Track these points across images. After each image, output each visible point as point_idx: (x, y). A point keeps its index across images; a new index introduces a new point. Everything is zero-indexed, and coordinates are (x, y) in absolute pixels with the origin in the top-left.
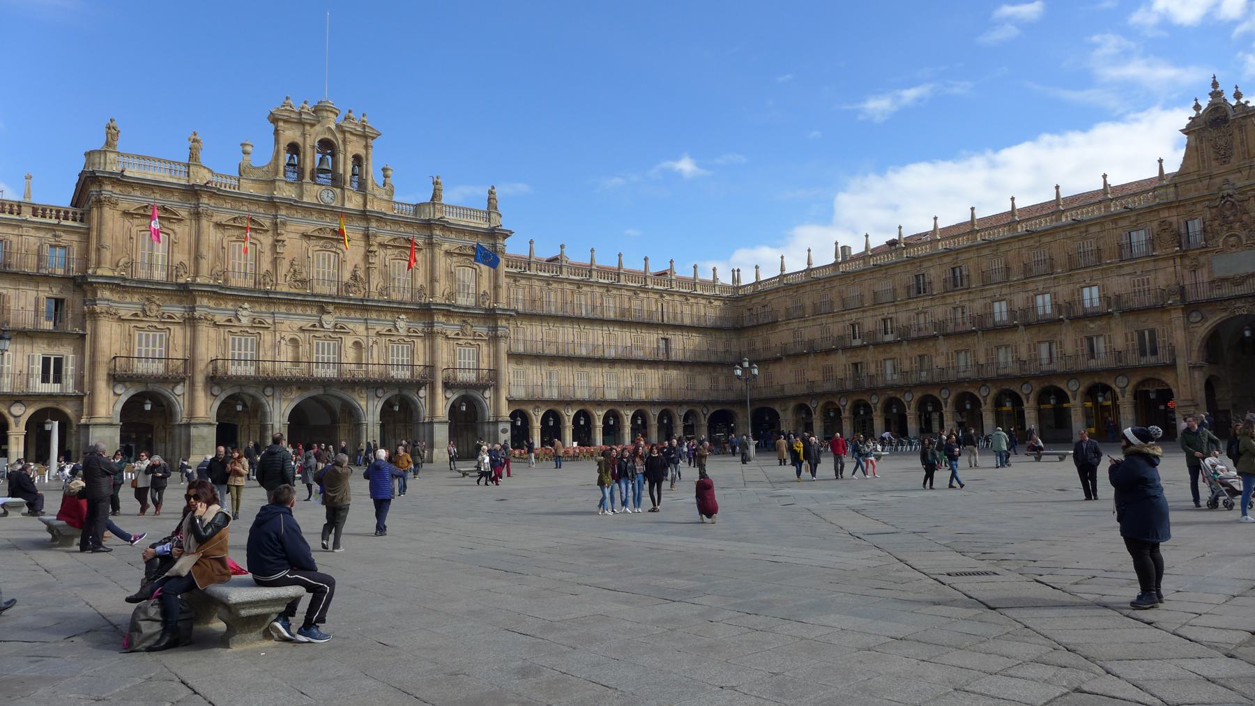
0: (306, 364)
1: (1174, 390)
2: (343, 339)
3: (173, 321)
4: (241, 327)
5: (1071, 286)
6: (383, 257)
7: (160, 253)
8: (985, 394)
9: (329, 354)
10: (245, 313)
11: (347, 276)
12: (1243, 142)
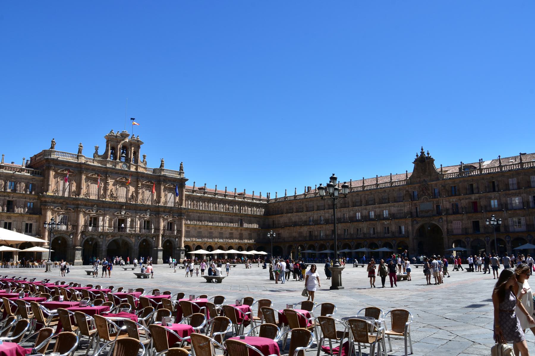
5: (380, 209)
8: (353, 244)
10: (95, 208)
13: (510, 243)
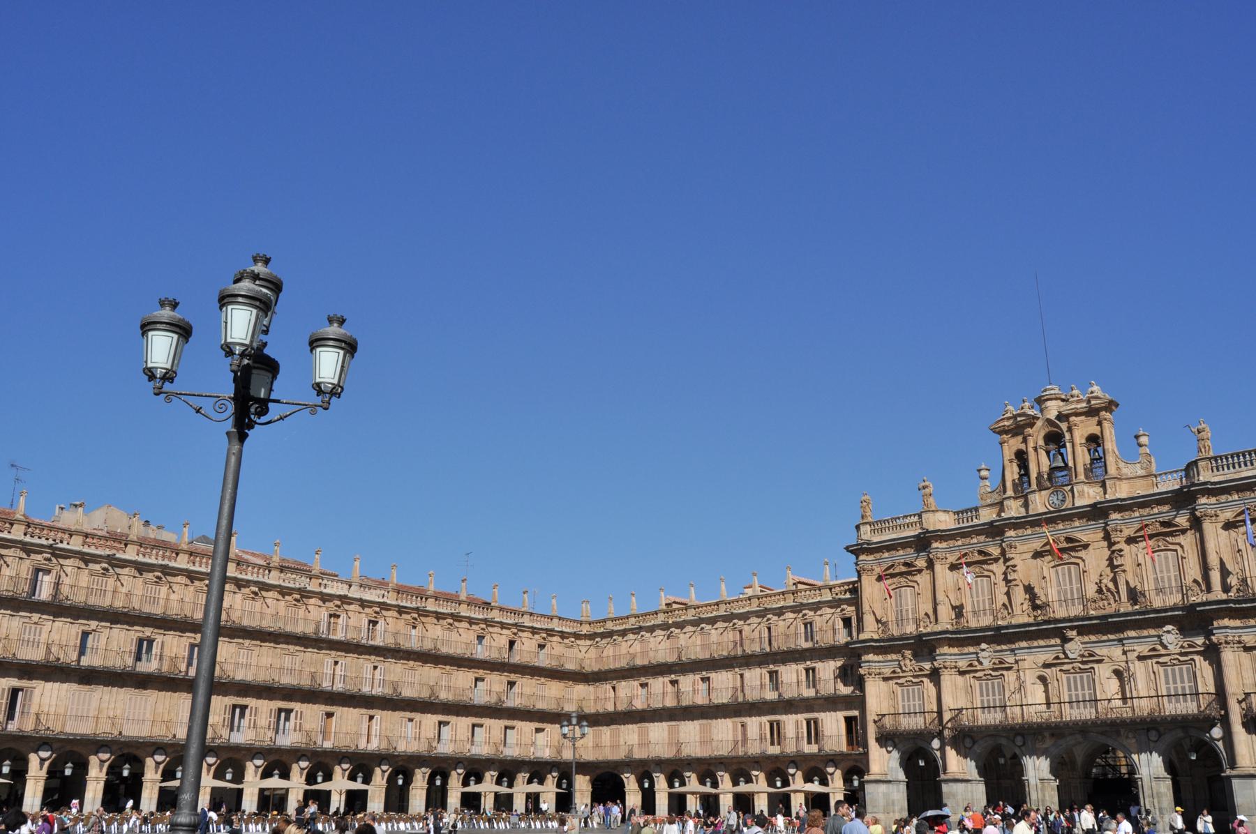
0: (1056, 705)
2: (1096, 670)
3: (923, 673)
4: (984, 670)
6: (1130, 555)
7: (910, 608)
9: (1083, 689)
11: (1091, 591)
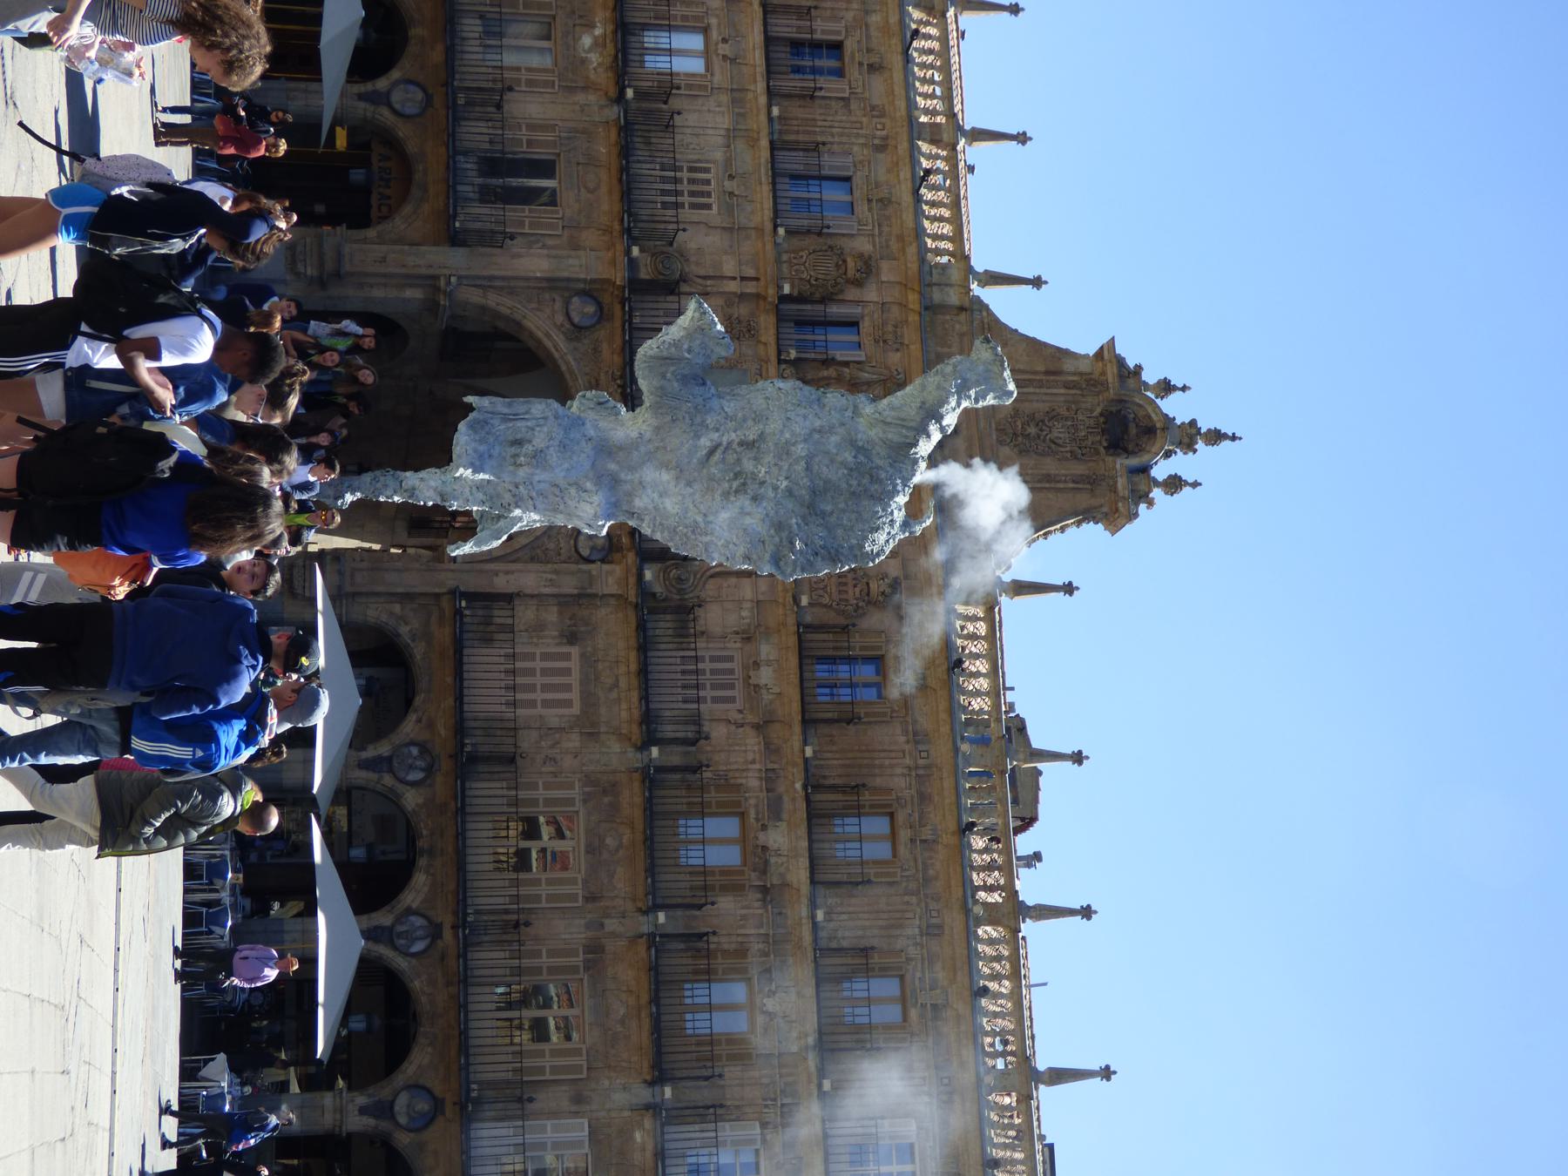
1: (371, 233)
12: (1048, 482)
13: (367, 1123)
